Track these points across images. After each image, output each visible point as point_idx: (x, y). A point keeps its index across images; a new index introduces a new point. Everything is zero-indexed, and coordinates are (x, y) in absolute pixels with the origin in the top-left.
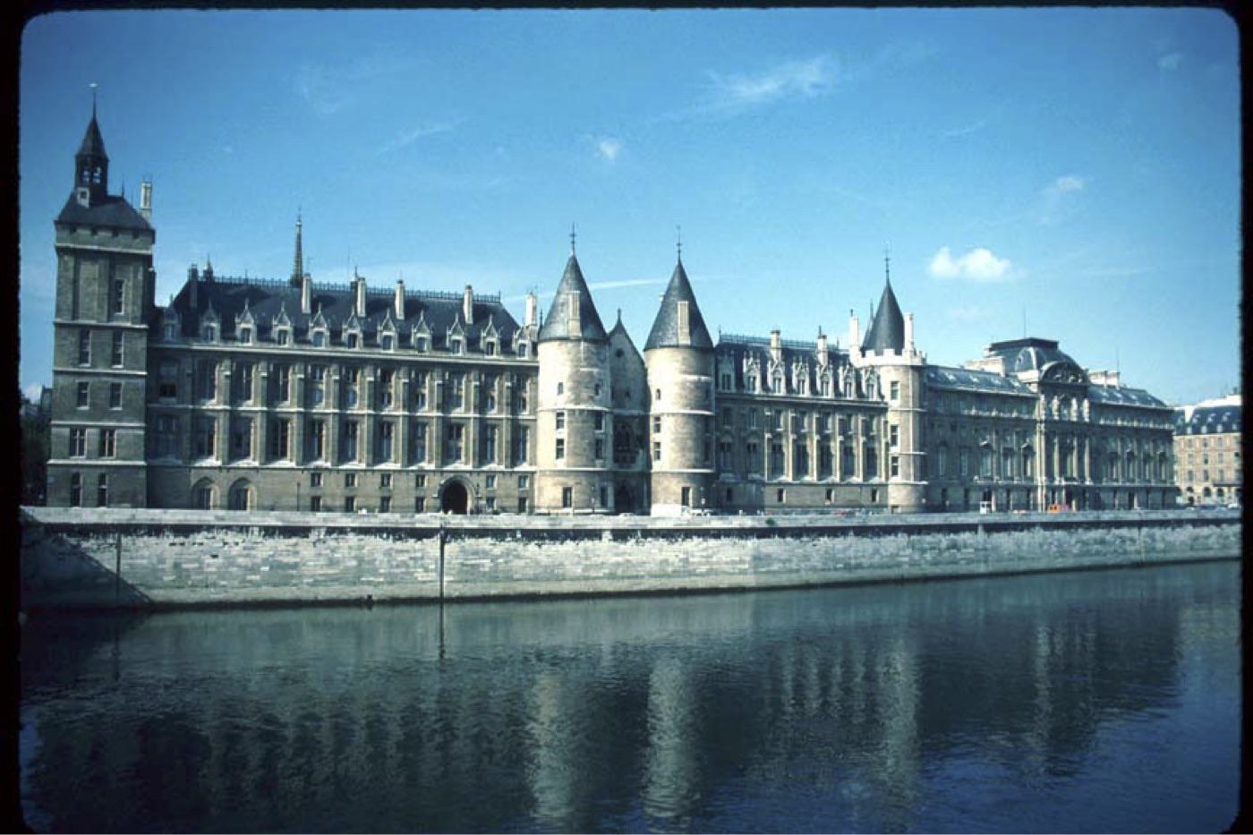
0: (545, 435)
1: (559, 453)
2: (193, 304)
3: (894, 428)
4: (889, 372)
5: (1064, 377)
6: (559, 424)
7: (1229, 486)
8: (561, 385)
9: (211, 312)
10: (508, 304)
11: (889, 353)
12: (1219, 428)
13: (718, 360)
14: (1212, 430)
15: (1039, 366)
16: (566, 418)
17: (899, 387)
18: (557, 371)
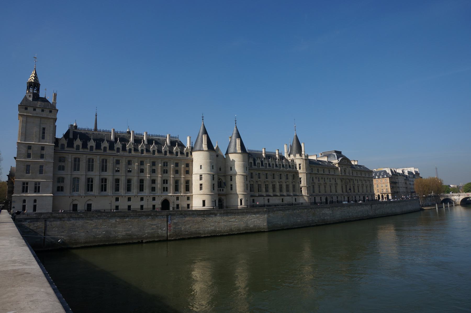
0: (195, 182)
1: (201, 188)
2: (71, 136)
3: (300, 178)
4: (298, 160)
5: (345, 161)
6: (201, 179)
7: (385, 194)
8: (201, 166)
9: (78, 139)
10: (180, 139)
11: (298, 156)
12: (381, 177)
13: (251, 159)
14: (379, 178)
15: (338, 159)
16: (203, 176)
17: (301, 165)
18: (200, 162)
